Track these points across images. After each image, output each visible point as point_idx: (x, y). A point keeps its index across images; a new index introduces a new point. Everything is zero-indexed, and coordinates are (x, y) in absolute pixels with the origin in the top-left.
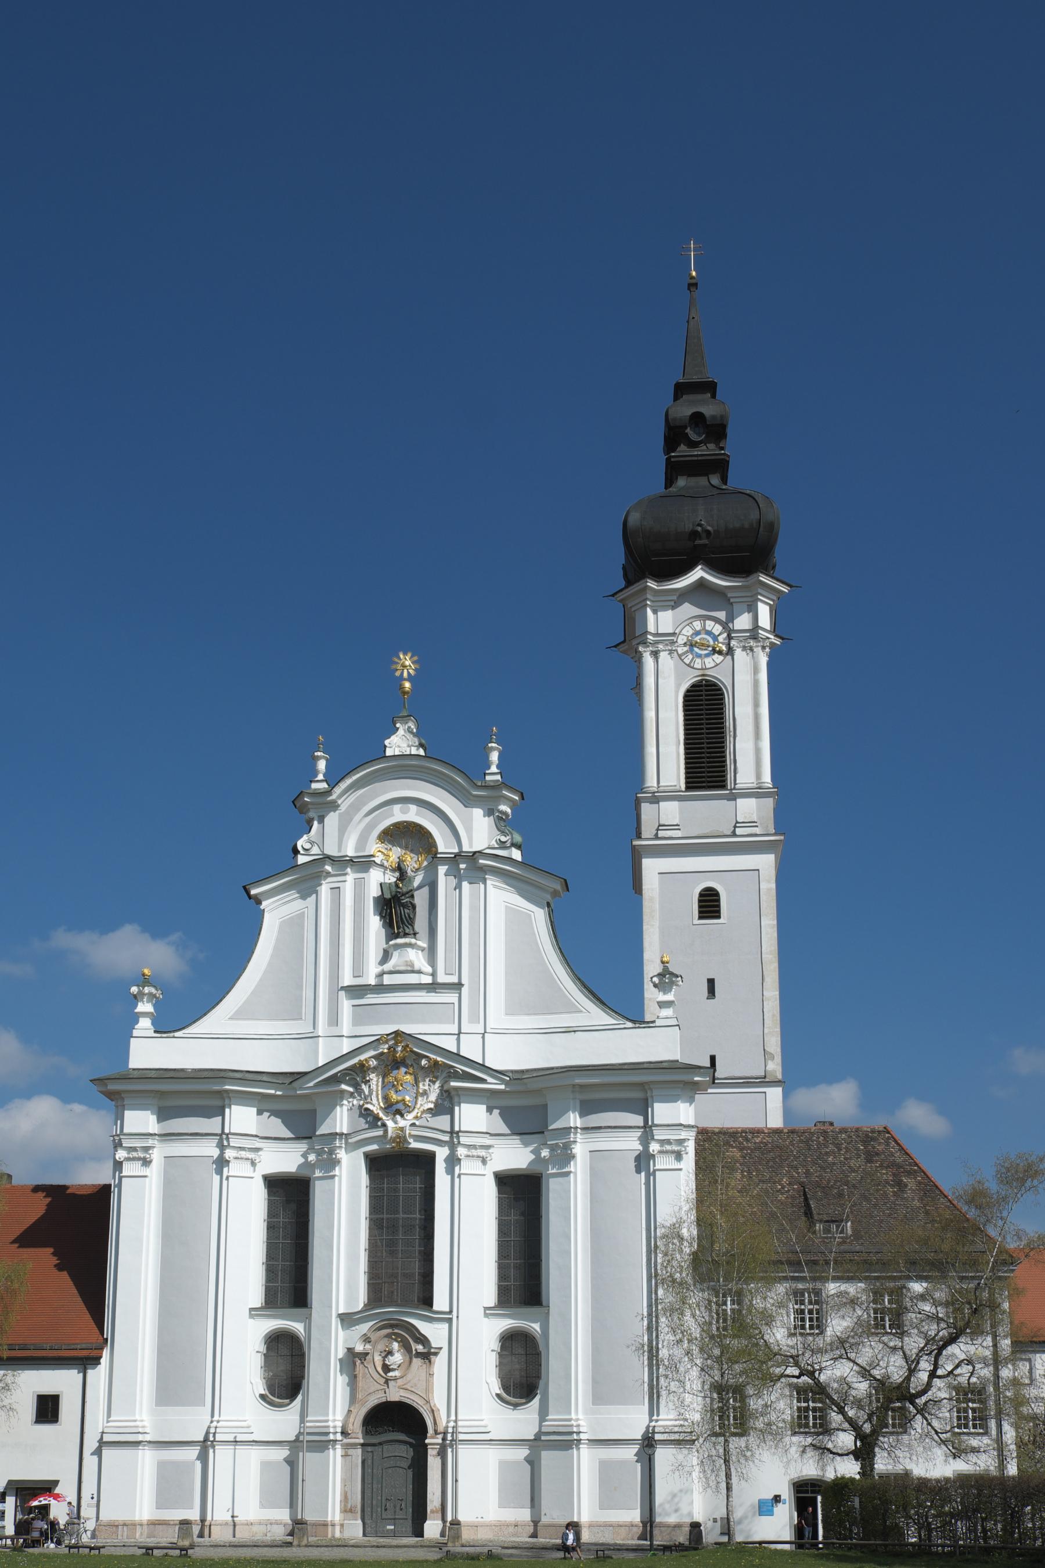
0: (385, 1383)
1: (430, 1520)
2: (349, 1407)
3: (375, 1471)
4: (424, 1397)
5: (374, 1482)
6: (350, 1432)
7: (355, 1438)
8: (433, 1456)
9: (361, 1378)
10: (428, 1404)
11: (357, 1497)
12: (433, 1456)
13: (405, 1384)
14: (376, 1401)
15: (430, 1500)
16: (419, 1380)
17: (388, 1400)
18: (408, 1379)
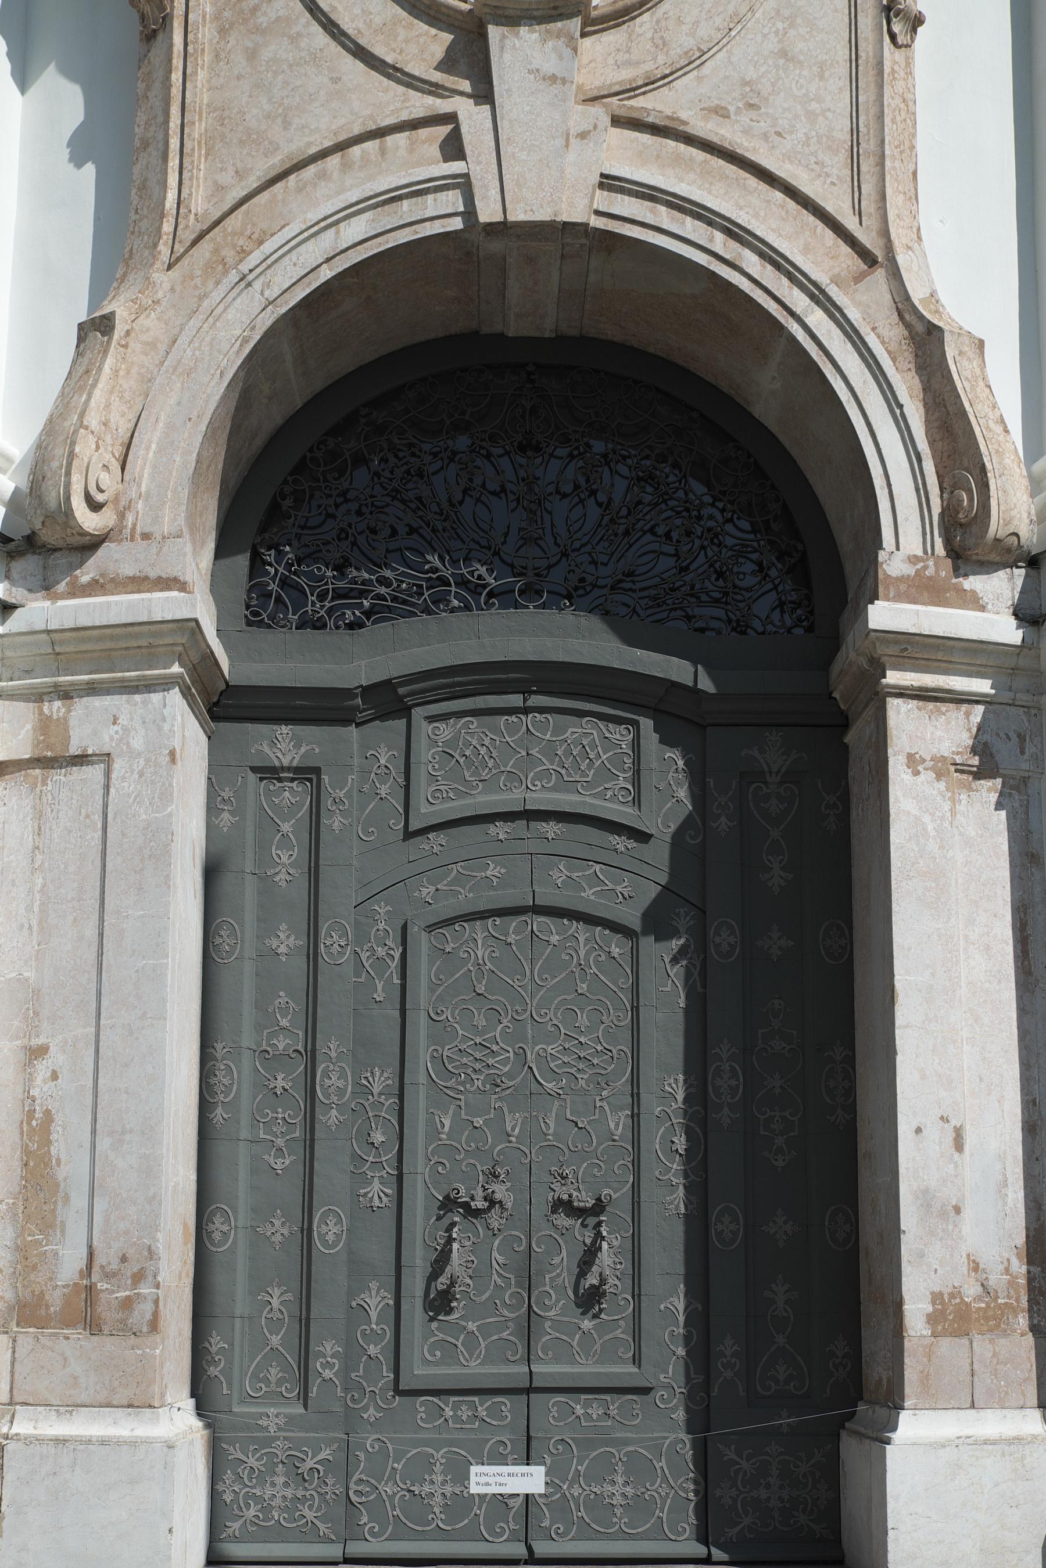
0: (447, 65)
1: (934, 1403)
2: (99, 290)
3: (331, 941)
4: (838, 206)
5: (331, 1047)
6: (89, 521)
7: (139, 583)
8: (942, 768)
9: (205, 34)
10: (880, 274)
11: (150, 1169)
12: (942, 768)
13: (651, 83)
14: (356, 229)
15: (926, 1198)
16: (783, 53)
17: (488, 212)
18: (683, 42)
